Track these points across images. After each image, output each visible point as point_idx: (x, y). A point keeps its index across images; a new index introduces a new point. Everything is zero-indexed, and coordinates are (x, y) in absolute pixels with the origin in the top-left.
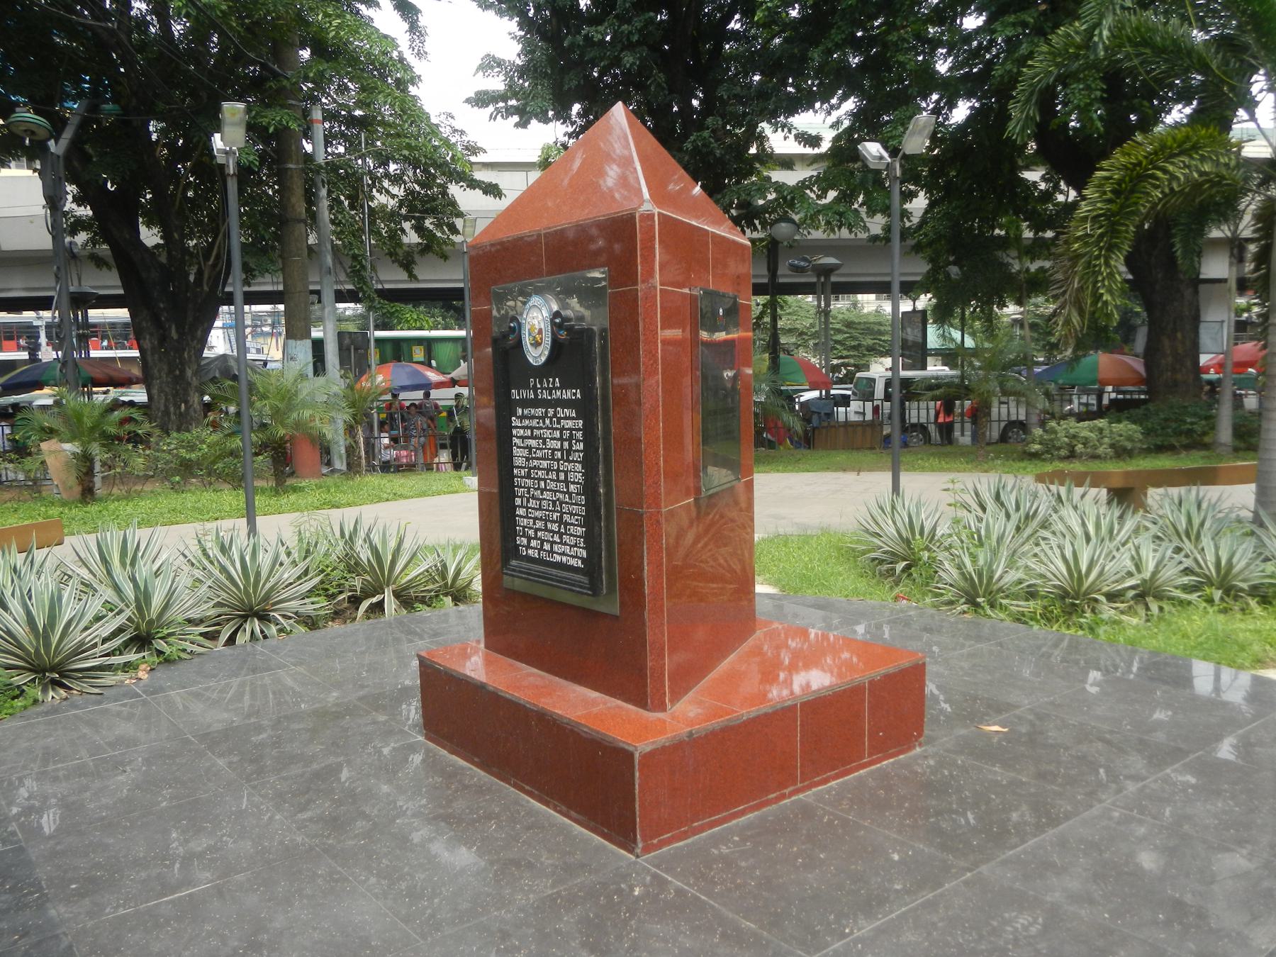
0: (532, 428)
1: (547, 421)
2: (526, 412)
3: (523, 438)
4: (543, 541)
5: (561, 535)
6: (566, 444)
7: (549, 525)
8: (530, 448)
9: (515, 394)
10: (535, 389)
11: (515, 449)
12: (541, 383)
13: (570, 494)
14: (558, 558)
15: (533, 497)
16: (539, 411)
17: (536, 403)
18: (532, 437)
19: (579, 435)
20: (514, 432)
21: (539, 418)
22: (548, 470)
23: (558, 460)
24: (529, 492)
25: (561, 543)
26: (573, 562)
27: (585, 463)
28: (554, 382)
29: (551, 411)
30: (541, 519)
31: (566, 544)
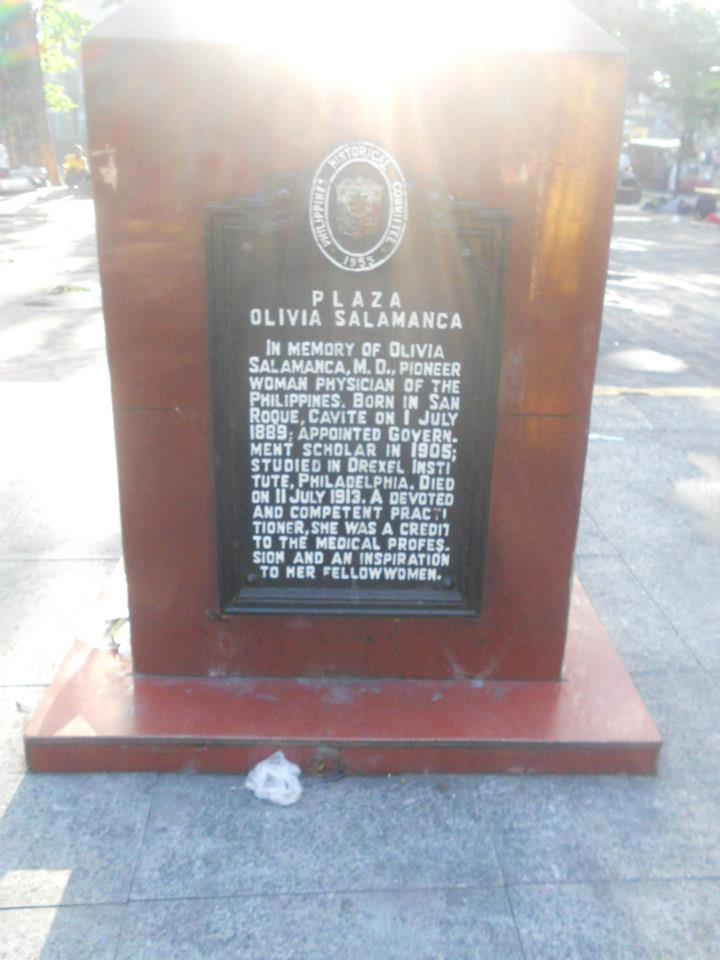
0: (312, 378)
1: (360, 366)
2: (293, 349)
3: (282, 393)
4: (328, 554)
5: (382, 540)
6: (414, 402)
7: (350, 527)
8: (303, 412)
10: (326, 309)
11: (254, 414)
12: (346, 300)
13: (414, 479)
14: (375, 574)
15: (306, 487)
16: (336, 348)
17: (326, 333)
18: (311, 390)
19: (454, 386)
20: (255, 383)
21: (335, 359)
22: (352, 445)
23: (384, 428)
24: (294, 477)
25: (384, 549)
26: (420, 574)
27: (456, 431)
28: (385, 301)
29: (370, 348)
30: (329, 519)
31: (395, 550)
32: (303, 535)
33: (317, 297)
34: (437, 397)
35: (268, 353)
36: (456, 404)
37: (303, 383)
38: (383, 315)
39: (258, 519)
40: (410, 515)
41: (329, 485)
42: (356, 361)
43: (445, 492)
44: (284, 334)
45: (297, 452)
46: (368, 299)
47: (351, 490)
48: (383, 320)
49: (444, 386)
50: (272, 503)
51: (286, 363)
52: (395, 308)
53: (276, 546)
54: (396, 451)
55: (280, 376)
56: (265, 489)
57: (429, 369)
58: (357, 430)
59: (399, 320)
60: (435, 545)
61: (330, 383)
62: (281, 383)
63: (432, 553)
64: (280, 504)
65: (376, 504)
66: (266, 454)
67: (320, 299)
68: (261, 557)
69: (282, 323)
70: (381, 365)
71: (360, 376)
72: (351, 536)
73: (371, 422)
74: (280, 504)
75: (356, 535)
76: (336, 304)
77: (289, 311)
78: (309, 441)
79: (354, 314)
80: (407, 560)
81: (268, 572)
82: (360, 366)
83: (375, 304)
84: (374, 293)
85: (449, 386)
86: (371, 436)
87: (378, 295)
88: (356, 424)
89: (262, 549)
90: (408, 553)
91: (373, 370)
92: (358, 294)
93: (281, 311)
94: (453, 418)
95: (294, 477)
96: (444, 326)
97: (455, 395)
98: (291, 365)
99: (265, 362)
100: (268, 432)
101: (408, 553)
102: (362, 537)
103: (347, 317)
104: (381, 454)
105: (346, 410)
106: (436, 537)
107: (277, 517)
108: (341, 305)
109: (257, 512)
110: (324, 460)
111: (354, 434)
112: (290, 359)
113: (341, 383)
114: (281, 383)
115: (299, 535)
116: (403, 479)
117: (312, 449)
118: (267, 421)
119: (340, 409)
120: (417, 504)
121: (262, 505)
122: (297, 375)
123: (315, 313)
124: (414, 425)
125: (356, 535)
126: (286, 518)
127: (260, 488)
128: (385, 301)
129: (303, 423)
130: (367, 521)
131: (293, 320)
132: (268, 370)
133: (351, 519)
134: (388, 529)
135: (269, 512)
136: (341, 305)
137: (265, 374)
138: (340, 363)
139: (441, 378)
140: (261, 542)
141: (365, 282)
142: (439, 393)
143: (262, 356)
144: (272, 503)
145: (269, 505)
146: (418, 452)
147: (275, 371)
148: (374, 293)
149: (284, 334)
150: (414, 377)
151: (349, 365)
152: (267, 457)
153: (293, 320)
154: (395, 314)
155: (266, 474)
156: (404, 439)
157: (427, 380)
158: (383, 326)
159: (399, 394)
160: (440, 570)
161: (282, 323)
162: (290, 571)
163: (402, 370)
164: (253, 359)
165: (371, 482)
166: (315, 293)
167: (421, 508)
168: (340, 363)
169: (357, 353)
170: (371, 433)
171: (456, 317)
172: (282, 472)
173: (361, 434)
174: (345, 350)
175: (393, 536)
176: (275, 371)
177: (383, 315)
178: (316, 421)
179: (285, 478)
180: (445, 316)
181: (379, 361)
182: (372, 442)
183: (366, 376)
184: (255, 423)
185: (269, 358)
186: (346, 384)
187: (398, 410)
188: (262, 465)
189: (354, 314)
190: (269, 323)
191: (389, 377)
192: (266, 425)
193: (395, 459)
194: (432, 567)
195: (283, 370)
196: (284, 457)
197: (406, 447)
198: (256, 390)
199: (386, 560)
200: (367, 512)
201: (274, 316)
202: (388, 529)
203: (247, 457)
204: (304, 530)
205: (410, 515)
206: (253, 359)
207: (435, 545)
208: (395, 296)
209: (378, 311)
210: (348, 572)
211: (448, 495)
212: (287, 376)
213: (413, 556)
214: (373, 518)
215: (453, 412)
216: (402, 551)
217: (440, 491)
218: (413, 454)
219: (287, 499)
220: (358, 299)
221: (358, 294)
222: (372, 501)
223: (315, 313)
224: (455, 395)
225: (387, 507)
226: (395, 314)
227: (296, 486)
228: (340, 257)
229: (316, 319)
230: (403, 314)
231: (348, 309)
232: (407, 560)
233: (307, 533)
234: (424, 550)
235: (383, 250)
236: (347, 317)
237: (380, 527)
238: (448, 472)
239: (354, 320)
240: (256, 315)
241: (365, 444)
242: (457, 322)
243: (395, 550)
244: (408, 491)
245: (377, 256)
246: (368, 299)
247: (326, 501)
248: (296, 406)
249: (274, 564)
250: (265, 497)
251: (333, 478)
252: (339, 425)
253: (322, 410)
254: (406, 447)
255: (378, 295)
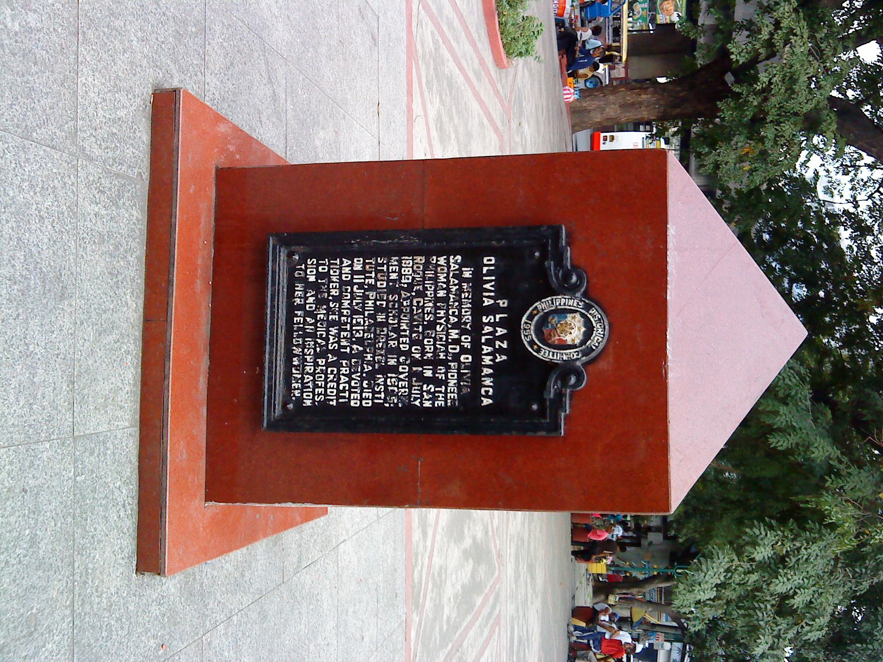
1: (454, 334)
6: (428, 374)
7: (333, 331)
8: (422, 294)
9: (489, 261)
10: (493, 310)
16: (467, 317)
17: (478, 310)
21: (460, 316)
22: (397, 330)
24: (373, 288)
25: (317, 356)
29: (467, 343)
31: (316, 365)
32: (329, 295)
33: (503, 303)
34: (432, 390)
35: (463, 269)
36: (427, 404)
37: (441, 294)
38: (490, 349)
39: (342, 262)
40: (343, 374)
41: (366, 313)
42: (457, 331)
43: (361, 399)
44: (477, 282)
45: (391, 290)
46: (501, 338)
47: (363, 330)
48: (486, 349)
49: (441, 395)
50: (354, 273)
51: (456, 282)
52: (496, 358)
53: (319, 275)
54: (392, 362)
55: (447, 277)
56: (364, 267)
57: (452, 382)
58: (407, 333)
59: (487, 360)
60: (319, 395)
61: (442, 313)
62: (442, 278)
63: (313, 392)
64: (352, 278)
65: (352, 349)
66: (391, 268)
67: (501, 305)
68: (312, 264)
69: (485, 278)
70: (455, 349)
71: (448, 335)
72: (328, 332)
73: (412, 343)
74: (352, 278)
75: (328, 334)
76: (498, 316)
77: (493, 283)
78: (399, 299)
79: (491, 329)
80: (308, 373)
81: (301, 269)
82: (454, 334)
83: (498, 343)
84: (505, 342)
85: (440, 398)
86: (403, 343)
87: (505, 346)
88: (411, 332)
89: (318, 265)
90: (313, 374)
91: (451, 344)
92: (505, 331)
93: (493, 278)
94: (417, 403)
95: (373, 288)
96: (483, 392)
97: (433, 404)
98: (455, 285)
99: (457, 267)
100: (407, 270)
101: (313, 374)
102: (327, 339)
103: (489, 324)
104: (390, 351)
105: (423, 325)
106: (326, 394)
107: (344, 276)
108: (497, 320)
109: (346, 262)
110: (385, 311)
111: (405, 331)
112: (459, 284)
113: (442, 321)
114: (442, 278)
115: (329, 293)
116: (371, 368)
117: (394, 301)
118: (415, 268)
119: (424, 320)
120: (351, 379)
121: (351, 265)
122: (448, 290)
123: (492, 302)
124: (411, 375)
125: (328, 334)
126: (342, 283)
127: (364, 264)
128: (501, 351)
129: (414, 294)
130: (338, 342)
131: (487, 286)
132: (452, 269)
133: (340, 330)
134: (331, 358)
135: (347, 270)
136: (497, 320)
137: (449, 267)
138: (456, 320)
139: (446, 393)
140: (324, 265)
141: (513, 336)
142: (435, 392)
143: (462, 265)
144: (354, 273)
145: (352, 270)
146: (391, 378)
147: (451, 275)
148: (505, 342)
149: (477, 282)
150: (446, 374)
151: (455, 326)
152: (388, 269)
153: (487, 286)
154: (491, 357)
155: (376, 268)
156: (401, 367)
157: (445, 383)
158: (483, 350)
159: (435, 363)
160: (301, 400)
161: (485, 278)
162: (300, 287)
163: (452, 364)
164: (459, 258)
165: (369, 345)
166: (506, 302)
167: (349, 382)
168: (456, 320)
169: (463, 332)
170: (405, 343)
171: (490, 401)
172: (377, 280)
173: (406, 336)
174: (466, 323)
175: (326, 361)
176: (451, 275)
177: (490, 349)
178: (415, 303)
179: (372, 281)
180: (490, 394)
181: (458, 347)
182: (399, 343)
183: (447, 338)
184: (413, 260)
185: (460, 269)
186: (441, 324)
187: (422, 363)
188: (382, 265)
189: (491, 329)
190: (485, 269)
191: (446, 356)
192: (412, 267)
193: (386, 362)
194: (302, 393)
195: (452, 280)
196: (389, 281)
197: (394, 369)
198: (437, 261)
199: (308, 358)
200: (344, 343)
201: (490, 273)
202: (331, 358)
203: (388, 253)
204: (333, 296)
205: (343, 374)
206: (459, 258)
207: (319, 395)
208: (504, 357)
209: (494, 346)
210: (299, 329)
211: (358, 402)
212: (448, 283)
213: (311, 378)
214: (340, 347)
215: (421, 403)
216: (315, 370)
217: (361, 396)
218: (389, 375)
219: (356, 284)
220: (500, 331)
221: (505, 331)
222: (355, 347)
223: (492, 302)
224: (433, 404)
225: (349, 357)
226: (491, 357)
227: (366, 290)
228: (531, 318)
229: (487, 302)
230: (491, 363)
231: (494, 325)
232: (308, 373)
233: (330, 298)
234: (317, 386)
235: (535, 347)
236: (489, 324)
237: (334, 352)
238: (376, 401)
239: (488, 329)
240: (490, 260)
241: (397, 339)
242: (486, 402)
243: (316, 365)
244: (362, 372)
245: (532, 343)
246: (501, 338)
247: (354, 312)
248: (426, 289)
249: (306, 274)
250: (358, 267)
251: (373, 316)
252: (412, 320)
253: (423, 307)
254: (394, 369)
255: (505, 346)
